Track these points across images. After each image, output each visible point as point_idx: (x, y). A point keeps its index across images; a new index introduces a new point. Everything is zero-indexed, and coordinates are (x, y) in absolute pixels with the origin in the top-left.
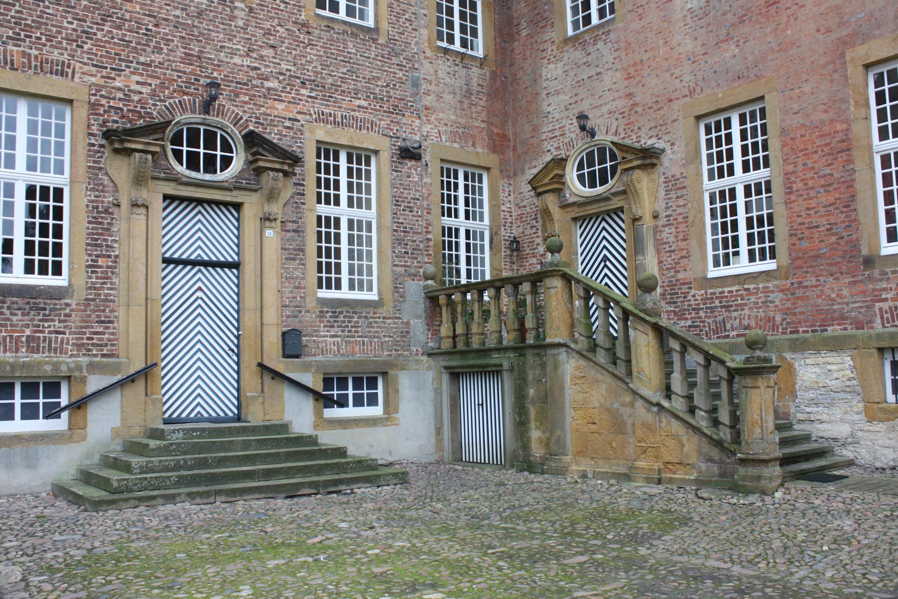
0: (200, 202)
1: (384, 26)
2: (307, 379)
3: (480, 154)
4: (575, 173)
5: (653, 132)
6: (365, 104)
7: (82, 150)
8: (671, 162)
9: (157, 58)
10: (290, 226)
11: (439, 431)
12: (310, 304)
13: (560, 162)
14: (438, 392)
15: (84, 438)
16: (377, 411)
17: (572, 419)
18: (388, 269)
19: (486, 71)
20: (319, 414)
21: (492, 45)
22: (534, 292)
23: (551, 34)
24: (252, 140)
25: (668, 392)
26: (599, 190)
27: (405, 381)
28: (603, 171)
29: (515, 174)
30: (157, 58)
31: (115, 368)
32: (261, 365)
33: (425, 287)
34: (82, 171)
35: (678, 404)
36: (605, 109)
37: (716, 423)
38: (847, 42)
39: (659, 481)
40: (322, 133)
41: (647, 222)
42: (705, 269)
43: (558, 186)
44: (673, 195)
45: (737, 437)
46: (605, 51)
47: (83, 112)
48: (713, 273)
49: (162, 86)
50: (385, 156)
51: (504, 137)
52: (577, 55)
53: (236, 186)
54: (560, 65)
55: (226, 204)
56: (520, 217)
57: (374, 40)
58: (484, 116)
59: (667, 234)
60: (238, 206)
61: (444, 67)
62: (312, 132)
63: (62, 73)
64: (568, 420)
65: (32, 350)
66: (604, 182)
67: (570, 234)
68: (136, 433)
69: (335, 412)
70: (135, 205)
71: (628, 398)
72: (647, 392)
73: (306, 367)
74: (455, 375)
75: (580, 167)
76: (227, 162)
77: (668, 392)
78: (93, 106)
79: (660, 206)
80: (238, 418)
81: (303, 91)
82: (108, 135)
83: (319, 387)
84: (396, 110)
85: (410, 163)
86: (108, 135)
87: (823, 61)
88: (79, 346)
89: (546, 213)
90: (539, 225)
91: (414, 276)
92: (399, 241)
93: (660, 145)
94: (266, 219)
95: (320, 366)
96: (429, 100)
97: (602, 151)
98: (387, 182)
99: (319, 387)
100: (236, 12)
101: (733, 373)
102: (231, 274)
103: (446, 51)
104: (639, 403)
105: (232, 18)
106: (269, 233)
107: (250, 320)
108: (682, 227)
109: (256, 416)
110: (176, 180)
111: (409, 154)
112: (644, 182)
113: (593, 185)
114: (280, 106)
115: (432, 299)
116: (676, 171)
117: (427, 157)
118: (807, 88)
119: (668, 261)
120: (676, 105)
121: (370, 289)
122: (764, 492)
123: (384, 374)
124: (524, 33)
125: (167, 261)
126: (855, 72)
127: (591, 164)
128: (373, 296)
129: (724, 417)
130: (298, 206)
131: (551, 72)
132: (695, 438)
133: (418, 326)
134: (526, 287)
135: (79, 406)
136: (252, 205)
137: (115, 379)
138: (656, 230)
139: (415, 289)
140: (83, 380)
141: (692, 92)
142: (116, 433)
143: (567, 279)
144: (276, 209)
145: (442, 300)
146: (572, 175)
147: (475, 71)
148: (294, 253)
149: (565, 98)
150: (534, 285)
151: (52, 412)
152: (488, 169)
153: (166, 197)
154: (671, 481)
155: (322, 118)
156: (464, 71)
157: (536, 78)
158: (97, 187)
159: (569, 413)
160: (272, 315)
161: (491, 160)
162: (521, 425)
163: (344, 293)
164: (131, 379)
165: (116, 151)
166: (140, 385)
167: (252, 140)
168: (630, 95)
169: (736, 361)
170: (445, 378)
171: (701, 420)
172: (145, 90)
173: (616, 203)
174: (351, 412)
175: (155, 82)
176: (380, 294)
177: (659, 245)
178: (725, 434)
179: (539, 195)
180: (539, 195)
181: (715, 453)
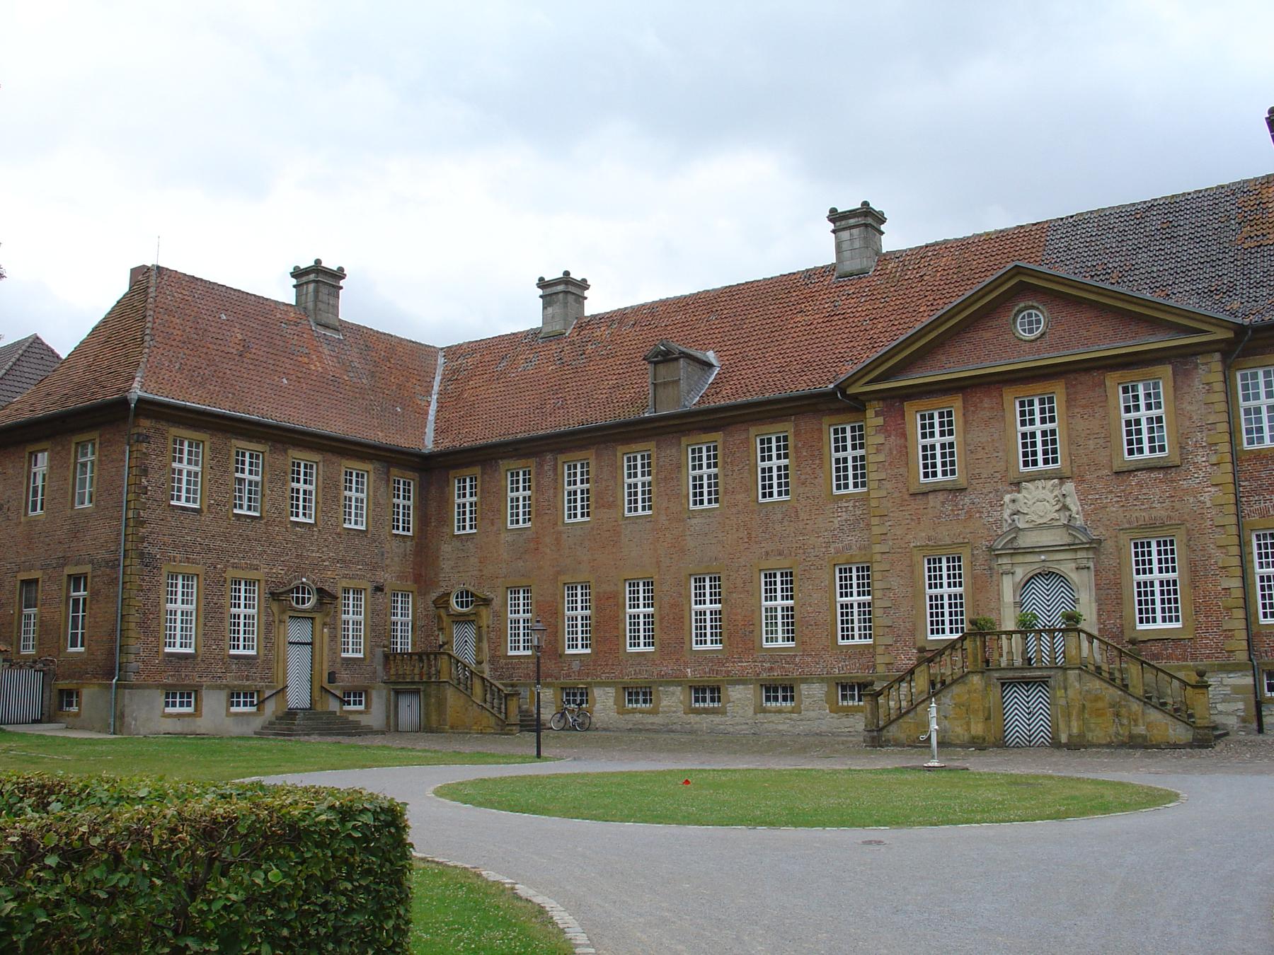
0: (299, 617)
1: (371, 528)
2: (338, 693)
3: (410, 585)
4: (454, 600)
5: (490, 590)
6: (361, 567)
7: (263, 600)
8: (496, 603)
9: (287, 558)
10: (332, 626)
11: (388, 717)
12: (338, 660)
13: (448, 594)
14: (388, 700)
15: (263, 715)
16: (362, 708)
17: (449, 711)
18: (368, 644)
19: (414, 542)
20: (341, 708)
21: (416, 529)
22: (435, 659)
23: (445, 530)
24: (320, 591)
25: (485, 701)
26: (465, 610)
27: (374, 694)
28: (467, 601)
29: (425, 595)
30: (287, 558)
31: (273, 688)
32: (322, 687)
33: (384, 651)
34: (262, 609)
35: (488, 706)
36: (469, 574)
37: (500, 712)
38: (558, 573)
39: (481, 733)
40: (345, 583)
41: (484, 629)
42: (507, 652)
43: (446, 605)
44: (495, 618)
45: (506, 718)
46: (471, 546)
47: (263, 584)
48: (510, 653)
49: (288, 570)
50: (369, 591)
51: (421, 575)
52: (459, 544)
53: (313, 610)
54: (450, 546)
55: (308, 618)
56: (427, 615)
57: (366, 536)
58: (412, 566)
59: (492, 635)
60: (312, 619)
61: (395, 543)
62: (341, 583)
63: (257, 569)
64: (448, 712)
65: (247, 680)
66: (467, 607)
67: (451, 629)
68: (279, 713)
69: (346, 708)
70: (280, 621)
71: (470, 703)
72: (478, 702)
73: (337, 688)
74: (397, 692)
75: (457, 597)
76: (309, 599)
77: (485, 701)
78: (267, 581)
79: (490, 622)
80: (310, 709)
81: (338, 565)
82: (272, 594)
83: (342, 697)
84: (374, 569)
85: (379, 593)
86: (272, 594)
87: (551, 577)
88: (261, 678)
89: (440, 617)
90: (436, 621)
91: (378, 646)
92: (373, 630)
93: (492, 596)
94: (325, 624)
95: (342, 688)
96: (388, 562)
97: (467, 592)
98: (369, 603)
99: (342, 697)
100: (314, 533)
101: (507, 695)
102: (309, 647)
103: (396, 535)
104: (475, 705)
105: (313, 536)
106: (325, 630)
107: (317, 666)
108: (498, 633)
109: (319, 708)
110: (294, 610)
111: (379, 589)
112: (484, 612)
113: (462, 607)
114: (329, 573)
115: (386, 657)
116: (497, 608)
117: (386, 589)
118: (545, 587)
119: (493, 646)
120: (499, 580)
121: (360, 652)
122: (513, 734)
123: (366, 692)
124: (433, 524)
125: (290, 643)
126: (560, 585)
127: (462, 597)
128: (361, 655)
129: (503, 710)
130: (335, 617)
131: (446, 548)
132: (494, 718)
133: (380, 668)
134: (432, 657)
135: (261, 703)
136: (319, 617)
137: (274, 691)
138: (488, 632)
139: (379, 651)
140: (264, 692)
141: (505, 577)
142: (274, 713)
143: (450, 656)
144: (328, 620)
145: (391, 658)
146: (453, 601)
147: (409, 543)
148: (333, 638)
149: (451, 563)
150: (436, 657)
151: (252, 704)
152: (412, 592)
153: (290, 617)
154: (485, 733)
155: (345, 576)
156: (402, 544)
157: (438, 549)
158: (268, 615)
159: (449, 709)
160: (325, 666)
161: (414, 587)
162: (427, 715)
163: (350, 655)
164: (278, 692)
165: (274, 600)
166: (281, 694)
167: (320, 591)
168: (480, 570)
169: (507, 690)
170: (392, 693)
171: (495, 711)
172: (282, 572)
173: (472, 618)
174: (352, 708)
175: (286, 568)
176: (364, 654)
177: (489, 639)
178: (503, 716)
179: (437, 608)
180: (437, 608)
181: (500, 723)
